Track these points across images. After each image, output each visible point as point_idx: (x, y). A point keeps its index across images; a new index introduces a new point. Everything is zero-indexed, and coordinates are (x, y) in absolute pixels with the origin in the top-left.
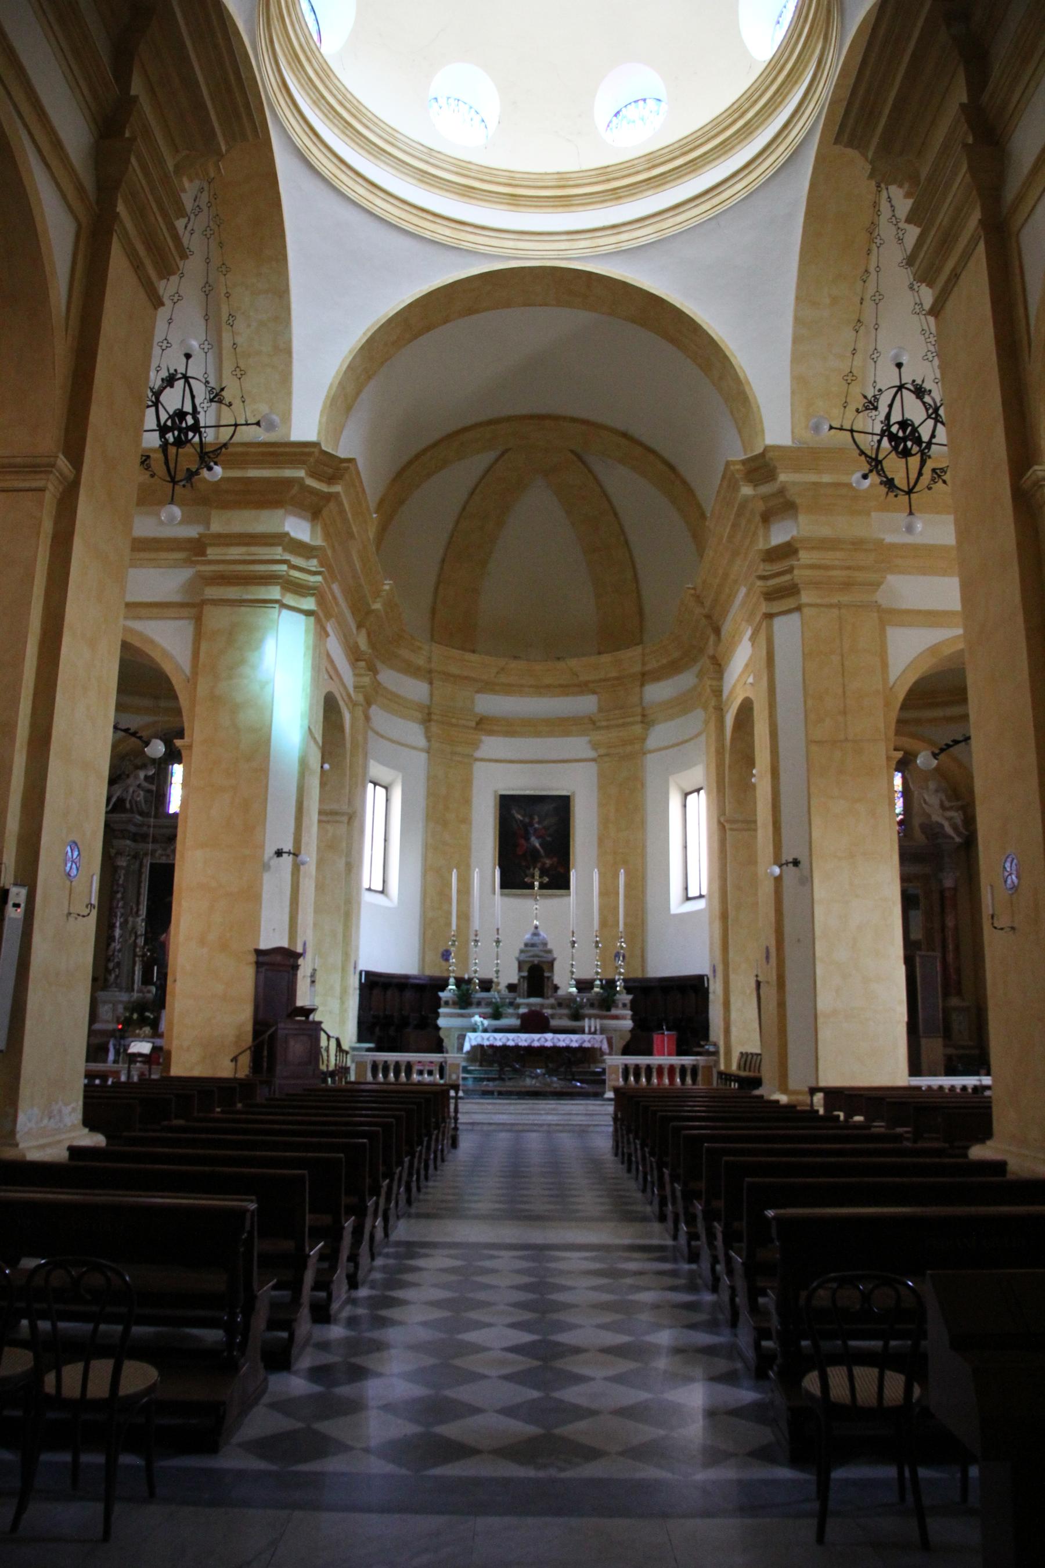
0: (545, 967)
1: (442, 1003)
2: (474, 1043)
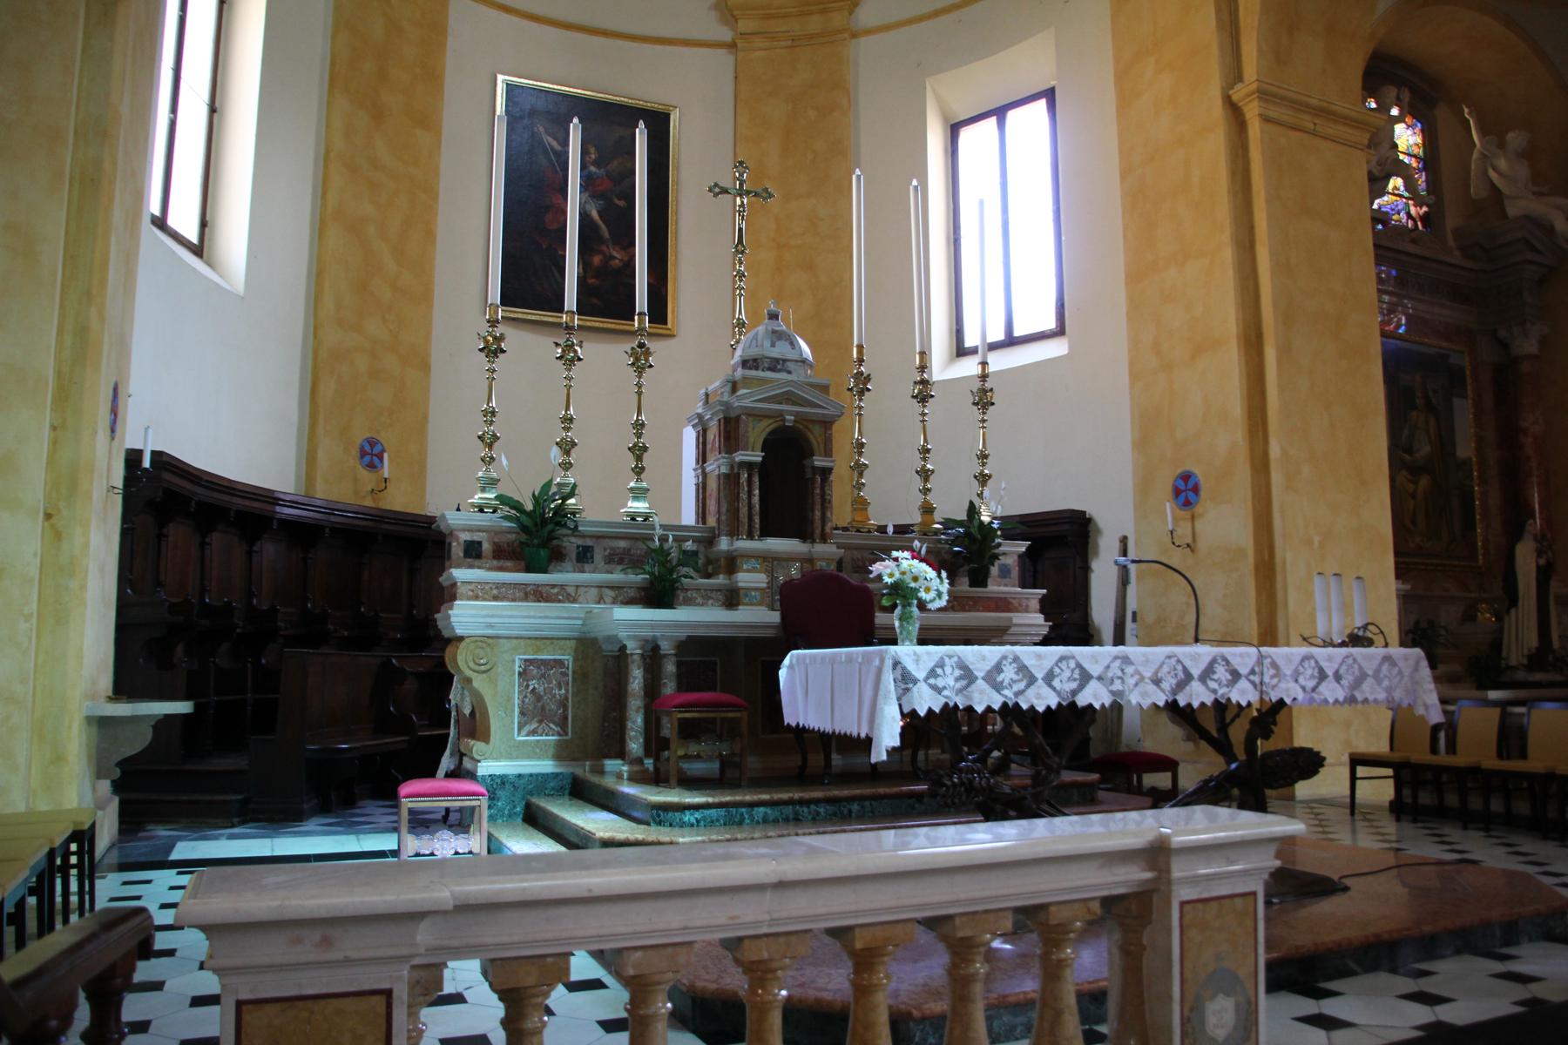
0: (815, 436)
1: (457, 550)
2: (925, 701)
